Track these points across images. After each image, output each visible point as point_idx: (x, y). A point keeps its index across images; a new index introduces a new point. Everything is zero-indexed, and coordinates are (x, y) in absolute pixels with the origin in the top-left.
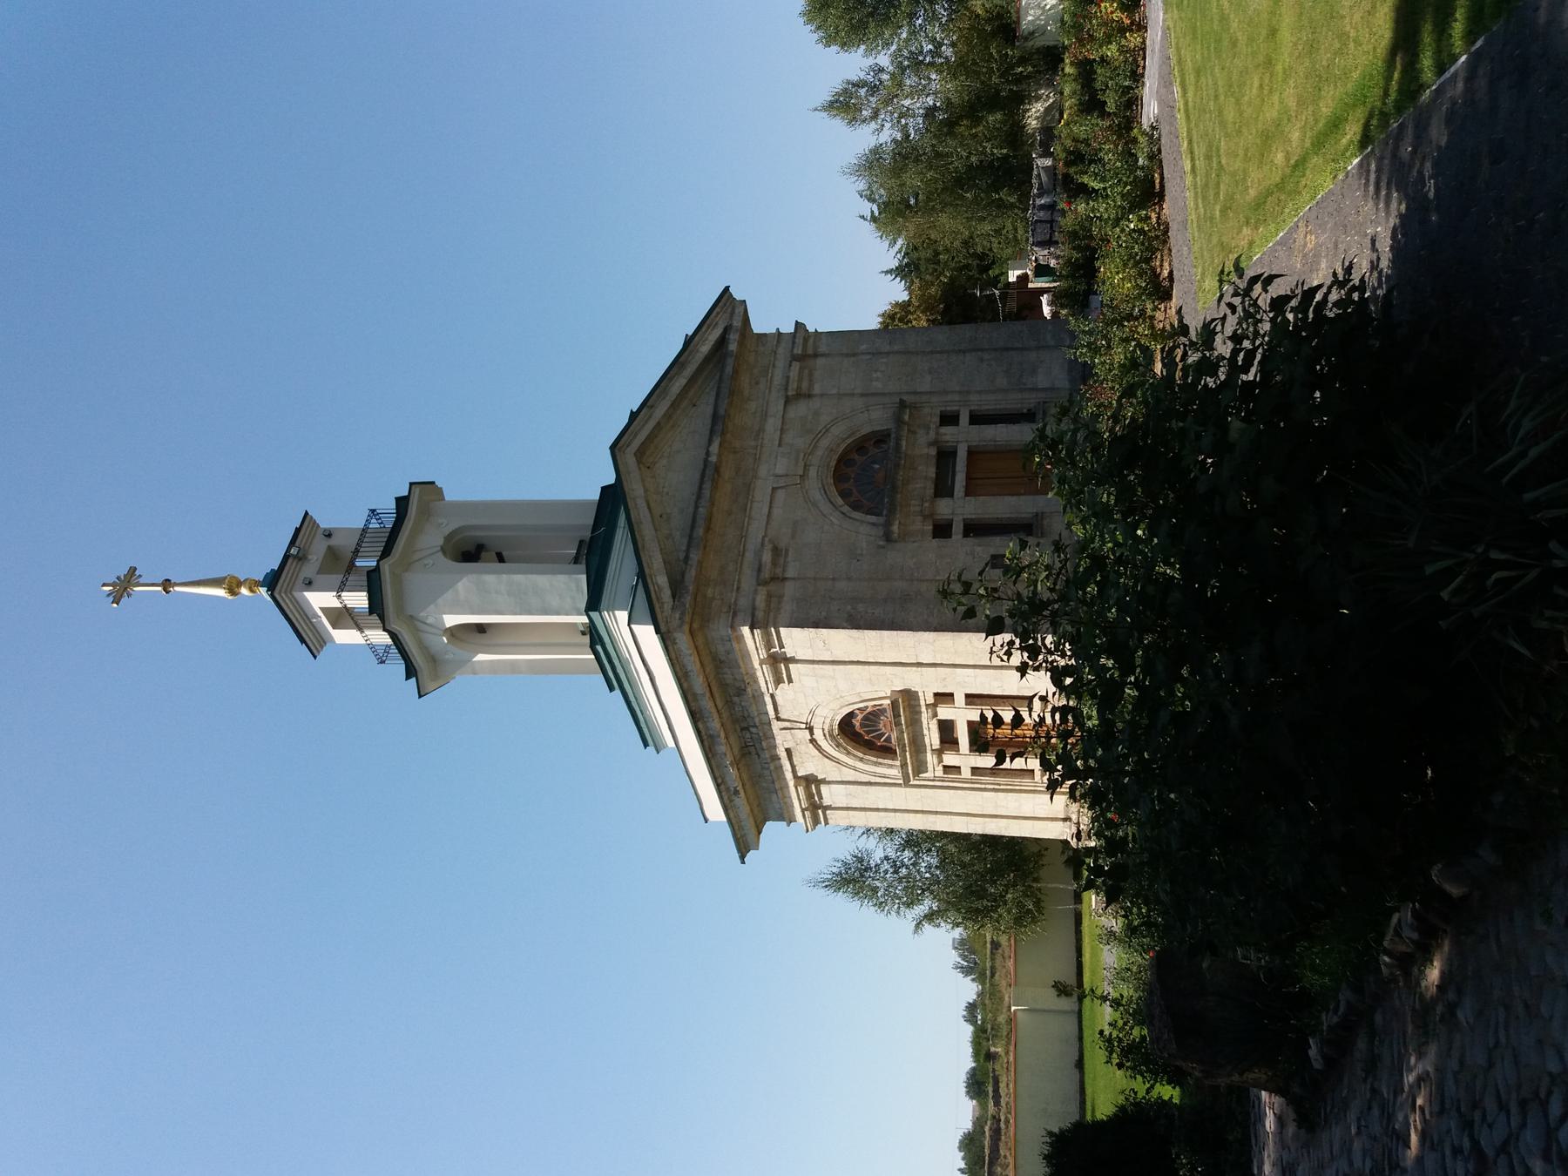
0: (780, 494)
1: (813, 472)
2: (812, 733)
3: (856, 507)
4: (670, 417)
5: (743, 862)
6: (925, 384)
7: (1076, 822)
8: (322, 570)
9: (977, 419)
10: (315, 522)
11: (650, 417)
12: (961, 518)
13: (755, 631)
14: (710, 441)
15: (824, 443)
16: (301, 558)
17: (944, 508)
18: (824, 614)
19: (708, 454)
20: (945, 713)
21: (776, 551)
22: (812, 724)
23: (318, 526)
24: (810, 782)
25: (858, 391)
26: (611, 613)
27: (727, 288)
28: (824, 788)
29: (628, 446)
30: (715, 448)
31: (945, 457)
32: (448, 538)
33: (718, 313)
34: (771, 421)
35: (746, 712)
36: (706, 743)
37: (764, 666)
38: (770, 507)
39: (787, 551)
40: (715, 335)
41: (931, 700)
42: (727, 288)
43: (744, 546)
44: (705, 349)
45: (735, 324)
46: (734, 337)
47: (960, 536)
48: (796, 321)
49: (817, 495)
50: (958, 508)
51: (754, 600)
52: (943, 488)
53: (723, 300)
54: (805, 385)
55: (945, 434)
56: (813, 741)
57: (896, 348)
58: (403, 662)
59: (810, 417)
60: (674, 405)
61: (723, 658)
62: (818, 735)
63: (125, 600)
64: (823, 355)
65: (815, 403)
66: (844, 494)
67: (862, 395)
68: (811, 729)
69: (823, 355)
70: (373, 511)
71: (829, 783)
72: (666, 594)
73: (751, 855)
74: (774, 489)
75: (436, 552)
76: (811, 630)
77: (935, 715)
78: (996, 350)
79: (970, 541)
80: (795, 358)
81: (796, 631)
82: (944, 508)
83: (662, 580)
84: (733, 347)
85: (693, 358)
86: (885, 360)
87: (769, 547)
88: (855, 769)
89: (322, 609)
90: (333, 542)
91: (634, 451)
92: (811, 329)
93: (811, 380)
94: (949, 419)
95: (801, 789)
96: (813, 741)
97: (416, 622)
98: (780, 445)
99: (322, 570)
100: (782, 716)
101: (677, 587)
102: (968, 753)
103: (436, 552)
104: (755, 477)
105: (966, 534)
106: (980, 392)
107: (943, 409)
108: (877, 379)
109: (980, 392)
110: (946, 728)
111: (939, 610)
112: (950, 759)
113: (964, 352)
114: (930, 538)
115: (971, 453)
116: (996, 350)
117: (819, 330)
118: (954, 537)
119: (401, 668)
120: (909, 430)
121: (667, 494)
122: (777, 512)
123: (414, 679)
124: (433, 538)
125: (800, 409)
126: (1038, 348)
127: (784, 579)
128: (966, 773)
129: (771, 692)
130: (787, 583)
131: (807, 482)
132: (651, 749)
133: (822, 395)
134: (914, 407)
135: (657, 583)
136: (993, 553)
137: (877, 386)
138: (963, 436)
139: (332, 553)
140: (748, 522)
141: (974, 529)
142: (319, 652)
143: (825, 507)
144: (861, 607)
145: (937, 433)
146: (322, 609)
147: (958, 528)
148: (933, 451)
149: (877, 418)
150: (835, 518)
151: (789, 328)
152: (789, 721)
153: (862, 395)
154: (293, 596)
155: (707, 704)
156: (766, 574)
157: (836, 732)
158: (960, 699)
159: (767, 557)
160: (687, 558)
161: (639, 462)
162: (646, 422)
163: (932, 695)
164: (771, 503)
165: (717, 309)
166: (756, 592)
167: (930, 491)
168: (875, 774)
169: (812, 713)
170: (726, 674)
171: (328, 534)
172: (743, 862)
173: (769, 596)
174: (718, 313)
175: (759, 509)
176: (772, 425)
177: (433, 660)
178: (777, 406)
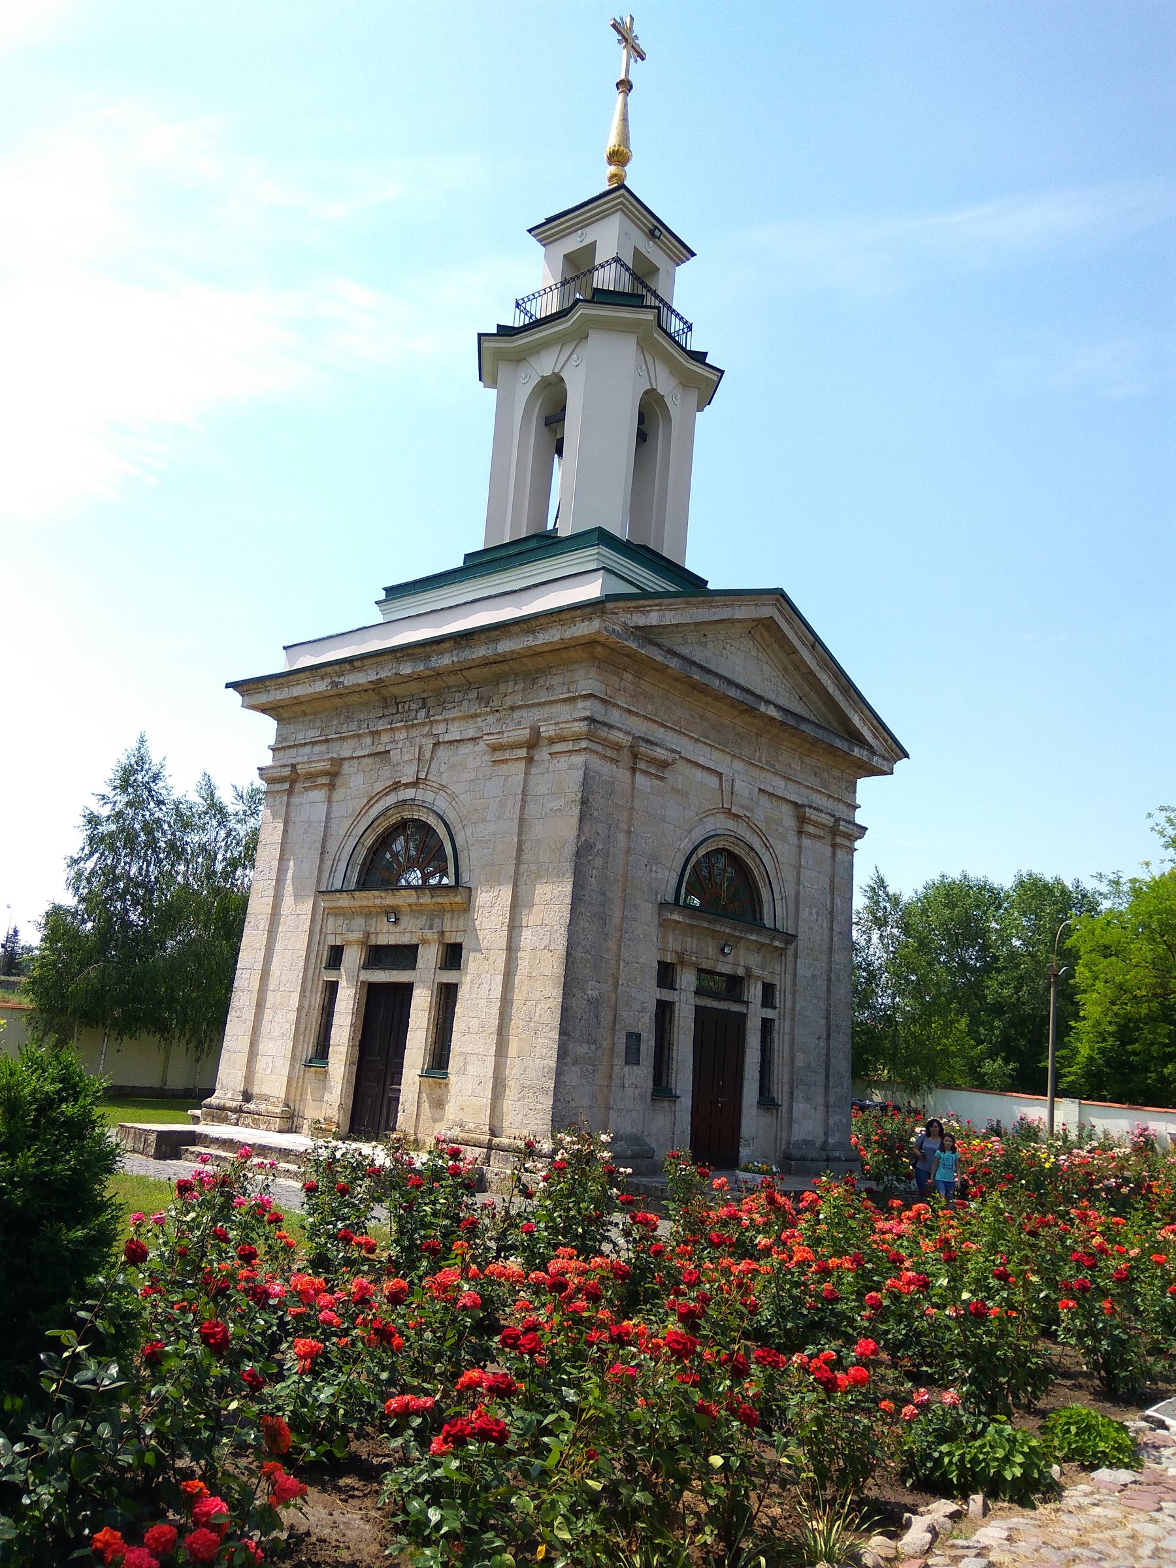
0: (713, 782)
1: (731, 824)
2: (406, 785)
4: (797, 668)
5: (228, 686)
7: (245, 1108)
10: (683, 262)
11: (804, 644)
12: (677, 999)
13: (586, 723)
14: (777, 707)
17: (687, 979)
18: (596, 814)
19: (768, 702)
20: (429, 956)
21: (664, 765)
22: (421, 786)
23: (678, 265)
24: (332, 777)
25: (802, 891)
26: (596, 557)
27: (907, 756)
28: (319, 795)
29: (779, 610)
30: (772, 712)
33: (886, 741)
34: (782, 783)
35: (452, 705)
36: (419, 650)
37: (528, 731)
38: (704, 768)
39: (662, 779)
41: (451, 939)
42: (907, 756)
43: (671, 728)
44: (856, 720)
45: (875, 758)
47: (658, 997)
48: (867, 829)
51: (620, 729)
53: (898, 751)
54: (810, 829)
55: (755, 988)
56: (396, 786)
57: (836, 939)
58: (522, 324)
59: (781, 830)
61: (541, 682)
62: (409, 793)
64: (834, 855)
65: (792, 839)
67: (797, 893)
68: (415, 784)
69: (834, 855)
70: (690, 328)
71: (329, 801)
72: (640, 620)
73: (235, 696)
75: (651, 382)
76: (580, 795)
77: (425, 942)
78: (827, 1055)
79: (652, 1007)
81: (579, 775)
82: (687, 979)
83: (653, 619)
84: (856, 752)
85: (850, 705)
86: (825, 925)
87: (669, 756)
88: (347, 835)
89: (593, 245)
91: (776, 619)
92: (858, 844)
93: (815, 836)
94: (768, 991)
95: (325, 766)
96: (396, 786)
97: (575, 343)
98: (760, 790)
100: (442, 752)
101: (645, 634)
102: (361, 979)
103: (651, 382)
106: (792, 1033)
107: (778, 987)
108: (811, 914)
109: (792, 1033)
110: (405, 956)
111: (588, 961)
112: (353, 957)
113: (827, 1018)
116: (827, 1055)
117: (855, 853)
119: (508, 322)
120: (763, 945)
121: (724, 648)
122: (699, 774)
123: (495, 331)
124: (666, 385)
125: (789, 821)
126: (827, 1105)
127: (634, 770)
128: (330, 976)
129: (485, 738)
130: (628, 774)
131: (722, 816)
132: (382, 595)
133: (800, 847)
134: (781, 952)
137: (805, 913)
140: (693, 737)
141: (664, 1010)
142: (535, 236)
143: (698, 834)
144: (599, 862)
145: (758, 978)
146: (593, 245)
147: (667, 995)
148: (741, 972)
149: (775, 911)
150: (686, 845)
151: (860, 818)
152: (432, 758)
153: (797, 893)
154: (615, 212)
155: (481, 652)
156: (644, 749)
157: (407, 815)
158: (449, 977)
159: (660, 753)
160: (674, 654)
161: (759, 621)
162: (800, 638)
163: (458, 941)
164: (709, 769)
165: (890, 741)
166: (628, 733)
167: (706, 965)
168: (337, 860)
169: (443, 787)
170: (516, 684)
172: (228, 686)
173: (618, 747)
174: (886, 741)
175: (703, 755)
176: (778, 785)
177: (519, 358)
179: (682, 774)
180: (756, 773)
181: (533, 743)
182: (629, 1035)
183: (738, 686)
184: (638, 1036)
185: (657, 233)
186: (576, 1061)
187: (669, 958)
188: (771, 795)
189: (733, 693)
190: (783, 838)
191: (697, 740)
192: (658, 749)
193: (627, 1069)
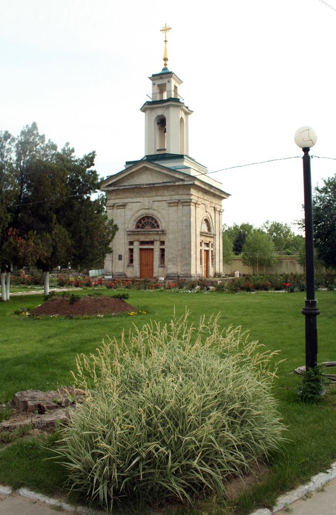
0: (140, 204)
1: (147, 211)
3: (140, 222)
6: (170, 237)
8: (159, 86)
9: (163, 250)
15: (155, 213)
16: (161, 78)
17: (136, 244)
31: (152, 243)
40: (181, 177)
44: (177, 176)
46: (181, 183)
49: (140, 213)
50: (136, 247)
52: (142, 243)
59: (163, 207)
60: (159, 172)
63: (162, 32)
66: (143, 219)
72: (107, 184)
79: (128, 250)
82: (136, 244)
90: (167, 85)
93: (172, 206)
98: (153, 201)
99: (159, 86)
104: (143, 197)
114: (129, 241)
115: (152, 249)
122: (135, 204)
125: (165, 204)
138: (157, 247)
139: (165, 84)
141: (131, 250)
147: (131, 247)
148: (152, 240)
149: (163, 225)
167: (141, 240)
171: (169, 82)
175: (135, 200)
176: (160, 198)
178: (165, 198)
179: (129, 206)
180: (151, 198)
181: (113, 206)
182: (119, 256)
183: (133, 185)
184: (121, 256)
186: (108, 260)
187: (131, 240)
188: (158, 201)
189: (132, 187)
190: (163, 209)
191: (132, 198)
193: (119, 261)
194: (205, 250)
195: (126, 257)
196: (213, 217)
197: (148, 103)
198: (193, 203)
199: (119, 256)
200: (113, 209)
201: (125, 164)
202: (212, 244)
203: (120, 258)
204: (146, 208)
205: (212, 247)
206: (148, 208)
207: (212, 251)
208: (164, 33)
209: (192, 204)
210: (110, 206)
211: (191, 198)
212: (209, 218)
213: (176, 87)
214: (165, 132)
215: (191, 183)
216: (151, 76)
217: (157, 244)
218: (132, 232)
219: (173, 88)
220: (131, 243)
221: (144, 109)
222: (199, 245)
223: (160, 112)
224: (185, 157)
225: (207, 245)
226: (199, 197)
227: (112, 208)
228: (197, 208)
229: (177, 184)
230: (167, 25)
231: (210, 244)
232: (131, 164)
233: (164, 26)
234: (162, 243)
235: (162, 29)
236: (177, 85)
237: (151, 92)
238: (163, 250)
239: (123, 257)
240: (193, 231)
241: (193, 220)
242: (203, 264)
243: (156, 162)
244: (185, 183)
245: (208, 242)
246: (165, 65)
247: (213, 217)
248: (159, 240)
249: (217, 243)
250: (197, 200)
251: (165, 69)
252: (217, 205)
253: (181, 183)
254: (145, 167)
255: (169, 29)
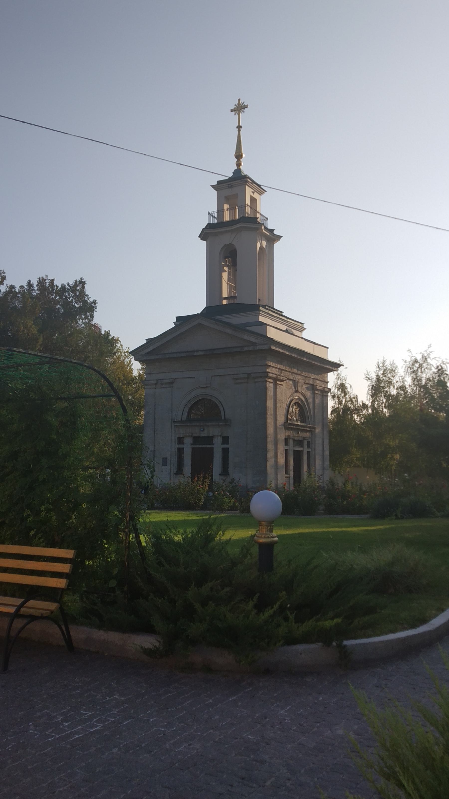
31: (210, 440)
32: (231, 245)
44: (246, 337)
51: (151, 380)
52: (196, 440)
63: (233, 113)
72: (147, 351)
74: (194, 377)
80: (249, 374)
83: (151, 348)
94: (225, 440)
98: (212, 376)
105: (179, 449)
114: (178, 436)
118: (178, 445)
135: (149, 347)
136: (168, 458)
140: (180, 371)
141: (180, 451)
148: (211, 435)
166: (154, 380)
167: (195, 435)
182: (163, 458)
183: (183, 352)
184: (167, 458)
185: (230, 186)
191: (182, 371)
192: (165, 380)
194: (294, 451)
195: (175, 460)
196: (310, 400)
197: (209, 226)
198: (271, 378)
199: (163, 458)
200: (155, 388)
201: (175, 321)
202: (309, 442)
203: (165, 462)
204: (201, 386)
205: (309, 447)
206: (205, 386)
207: (308, 453)
208: (237, 116)
209: (270, 380)
210: (152, 384)
211: (268, 371)
212: (302, 401)
213: (253, 200)
214: (236, 271)
215: (266, 347)
216: (216, 184)
217: (218, 441)
218: (181, 421)
219: (248, 202)
220: (180, 440)
221: (204, 236)
222: (284, 443)
223: (226, 239)
224: (261, 308)
225: (300, 443)
226: (282, 370)
227: (154, 386)
228: (278, 386)
229: (246, 349)
230: (241, 101)
231: (306, 442)
232: (181, 320)
233: (237, 103)
234: (225, 440)
235: (233, 107)
236: (256, 195)
237: (216, 209)
238: (225, 452)
239: (168, 461)
240: (270, 421)
241: (270, 404)
242: (292, 473)
243: (216, 318)
244: (258, 348)
245: (301, 439)
246: (239, 164)
247: (310, 400)
248: (221, 436)
249: (318, 441)
250: (278, 373)
251: (238, 172)
252: (318, 382)
253: (251, 348)
254: (199, 324)
255: (244, 108)
